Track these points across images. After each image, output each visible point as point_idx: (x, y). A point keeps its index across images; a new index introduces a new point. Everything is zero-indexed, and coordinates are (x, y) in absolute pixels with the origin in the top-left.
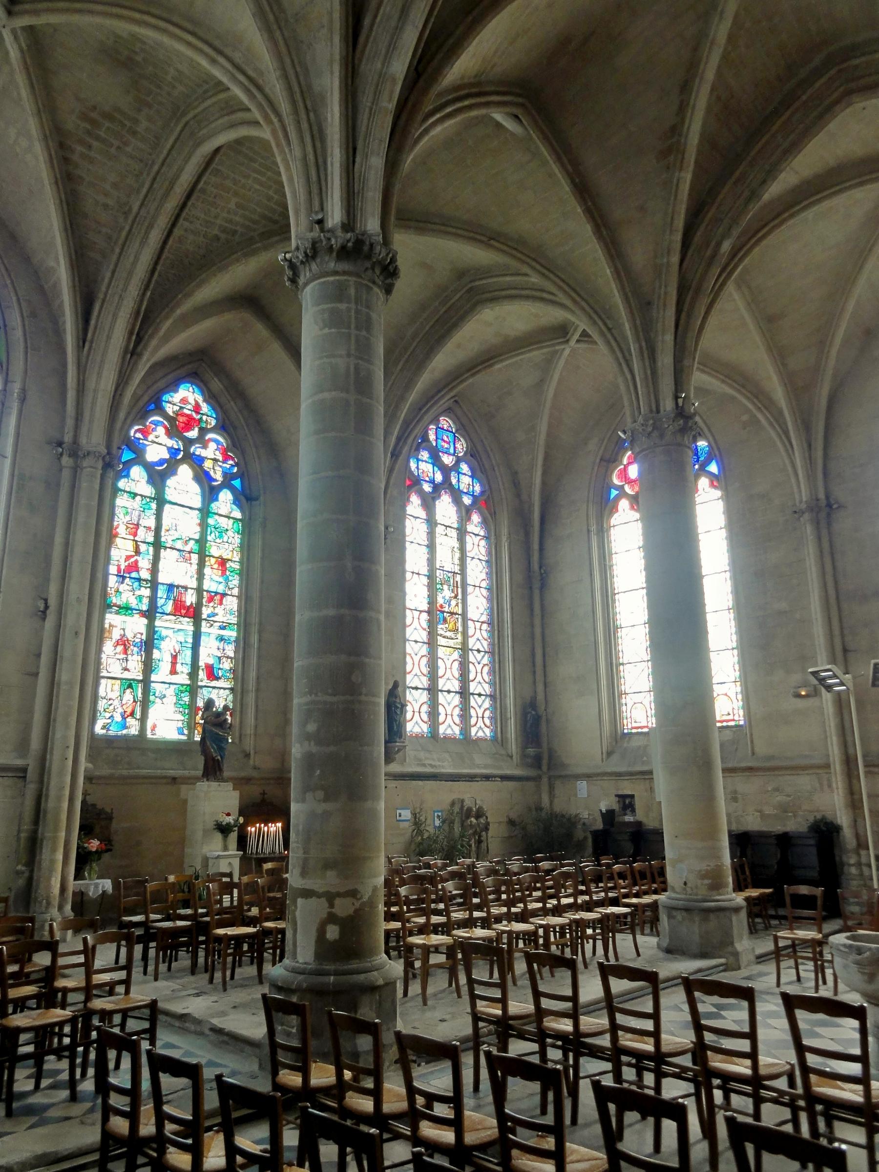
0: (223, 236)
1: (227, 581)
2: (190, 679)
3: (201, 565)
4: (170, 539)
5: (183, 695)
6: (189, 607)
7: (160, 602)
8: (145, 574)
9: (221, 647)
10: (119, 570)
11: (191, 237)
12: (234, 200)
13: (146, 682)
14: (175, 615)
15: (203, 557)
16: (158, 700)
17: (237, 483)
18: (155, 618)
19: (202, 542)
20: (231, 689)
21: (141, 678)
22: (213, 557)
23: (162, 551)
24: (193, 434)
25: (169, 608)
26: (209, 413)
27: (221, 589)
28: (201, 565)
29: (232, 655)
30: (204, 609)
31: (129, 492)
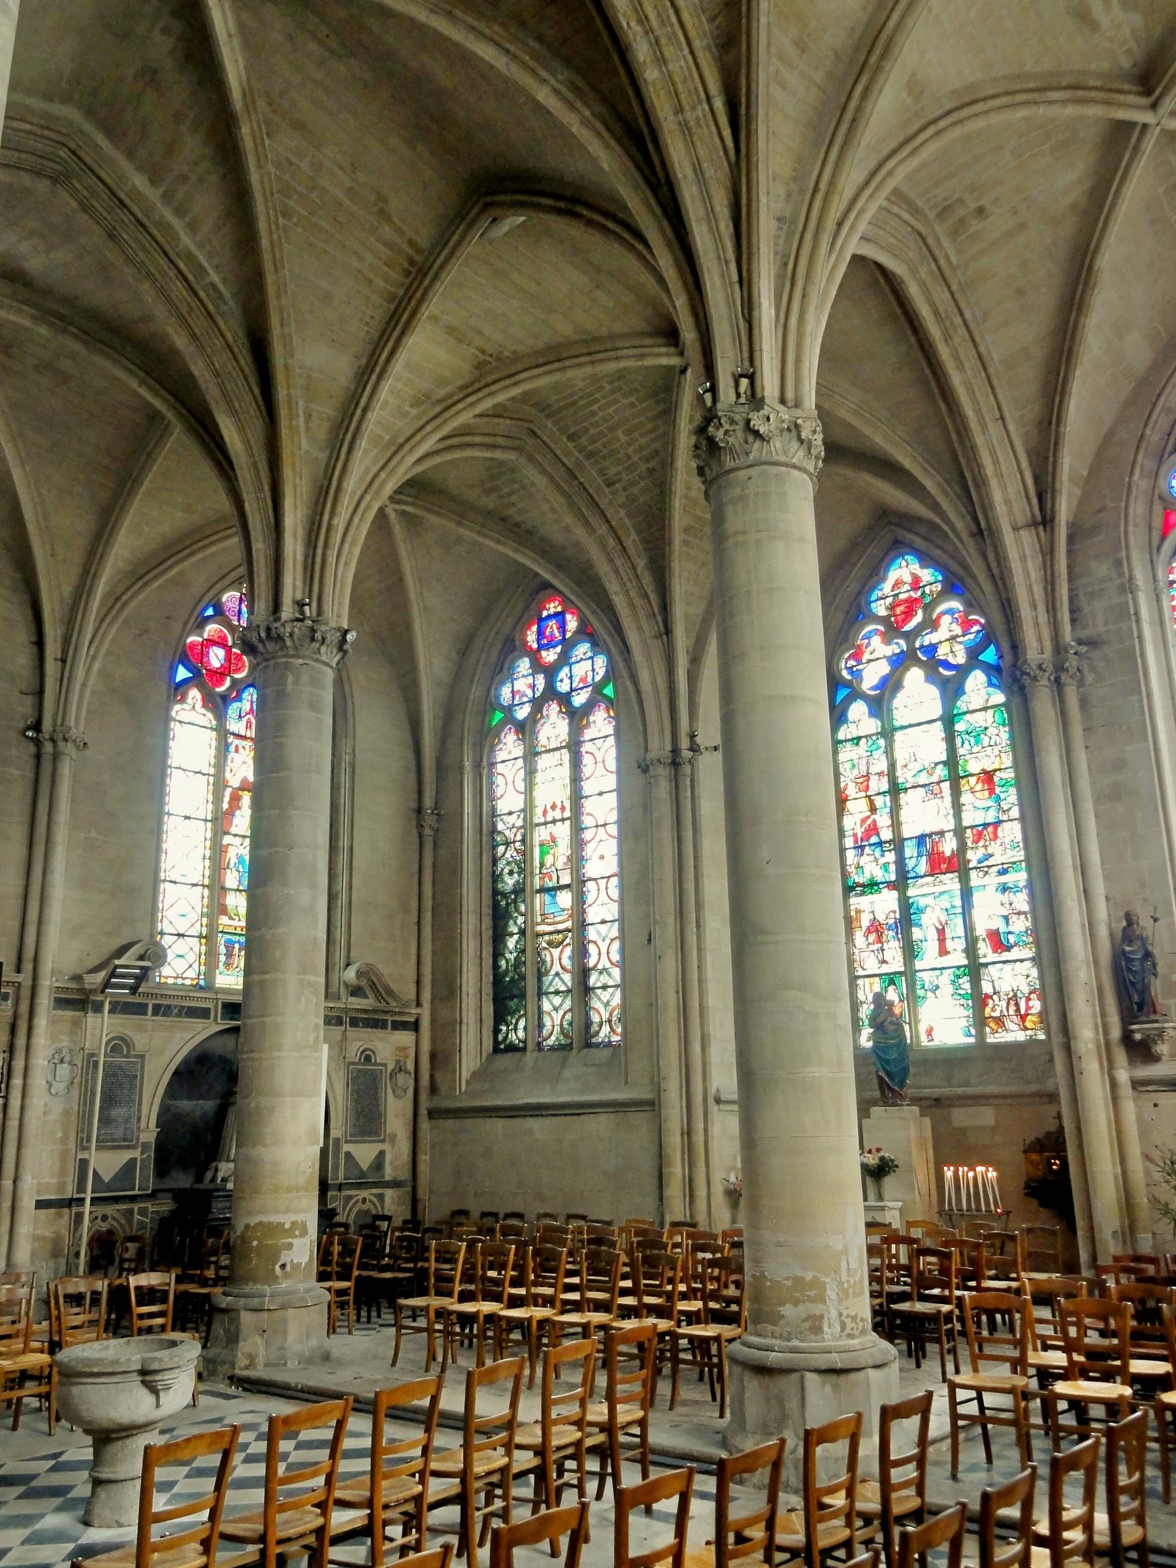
0: (653, 464)
1: (999, 800)
2: (968, 957)
3: (956, 792)
4: (909, 776)
5: (960, 981)
6: (950, 858)
7: (910, 863)
8: (886, 835)
9: (1006, 901)
10: (856, 842)
11: (635, 490)
12: (620, 433)
13: (909, 973)
14: (932, 875)
15: (955, 780)
16: (929, 994)
18: (906, 887)
19: (952, 761)
20: (1033, 959)
21: (902, 969)
22: (972, 775)
23: (902, 795)
24: (918, 618)
25: (923, 867)
26: (932, 579)
27: (991, 817)
28: (956, 792)
29: (1025, 907)
30: (970, 855)
31: (852, 739)
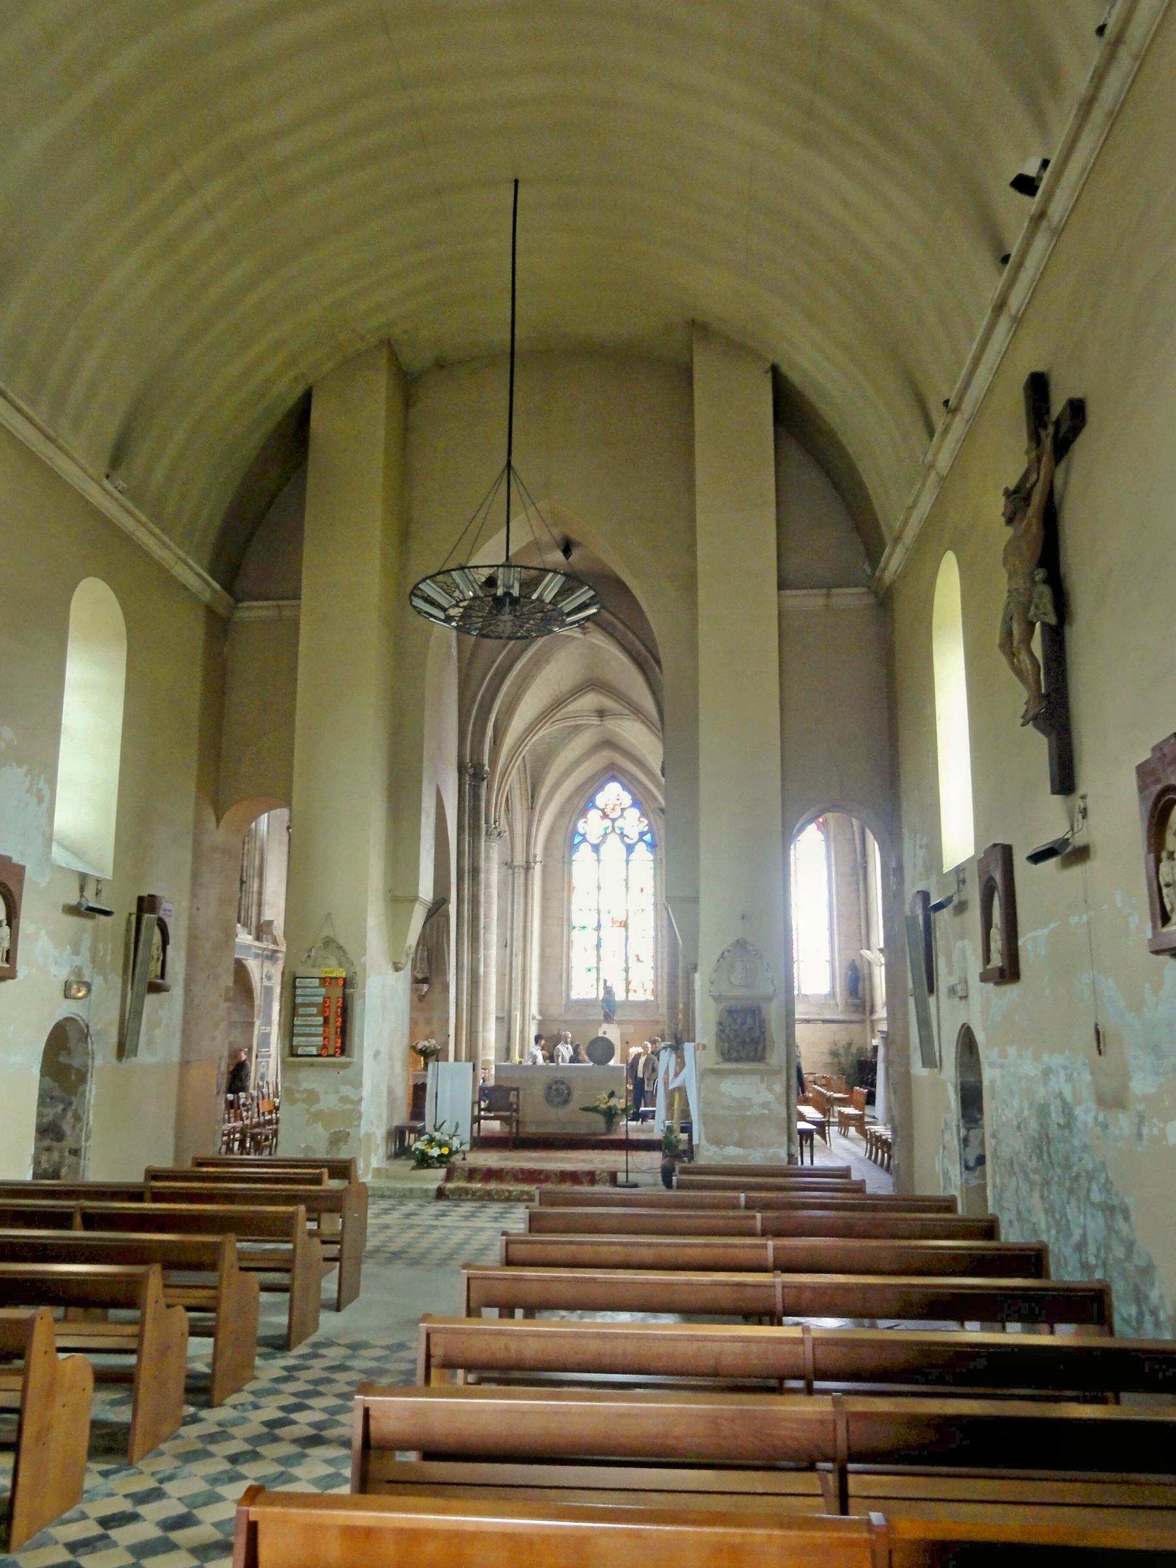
17: (648, 838)
